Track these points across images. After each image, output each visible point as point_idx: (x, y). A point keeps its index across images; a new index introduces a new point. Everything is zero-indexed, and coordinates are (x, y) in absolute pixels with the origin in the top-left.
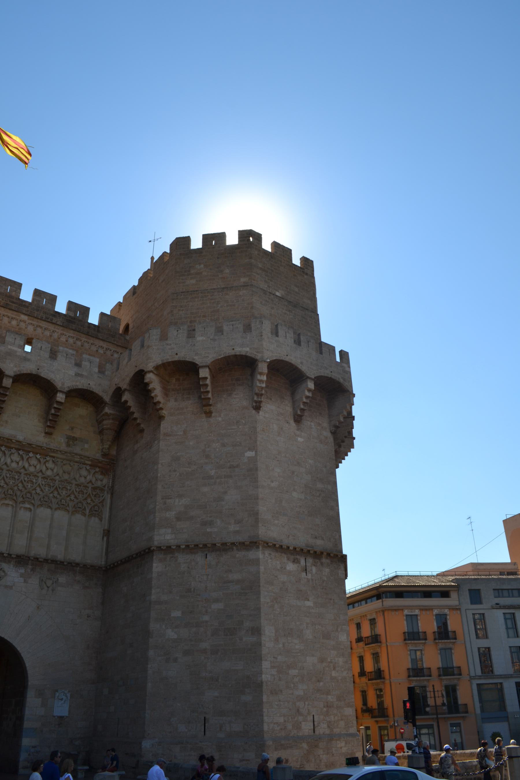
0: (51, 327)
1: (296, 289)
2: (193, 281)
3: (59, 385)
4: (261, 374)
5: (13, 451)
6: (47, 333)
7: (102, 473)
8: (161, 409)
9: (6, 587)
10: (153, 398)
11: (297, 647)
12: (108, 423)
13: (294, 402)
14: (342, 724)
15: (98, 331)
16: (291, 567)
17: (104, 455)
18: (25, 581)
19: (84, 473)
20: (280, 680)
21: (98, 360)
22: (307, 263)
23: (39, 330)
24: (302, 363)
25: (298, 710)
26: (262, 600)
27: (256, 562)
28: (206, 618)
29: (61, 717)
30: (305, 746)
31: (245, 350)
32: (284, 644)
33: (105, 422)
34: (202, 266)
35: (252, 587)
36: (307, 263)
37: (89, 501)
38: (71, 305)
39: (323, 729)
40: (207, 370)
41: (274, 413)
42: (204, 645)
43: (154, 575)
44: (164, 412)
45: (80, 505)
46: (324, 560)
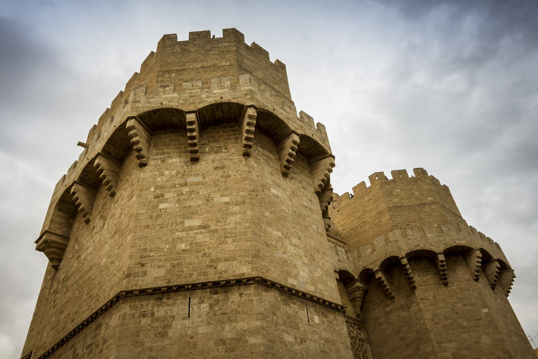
2: (398, 200)
7: (359, 329)
8: (414, 282)
10: (408, 274)
12: (359, 294)
13: (487, 277)
31: (463, 242)
33: (357, 293)
34: (399, 190)
44: (416, 284)
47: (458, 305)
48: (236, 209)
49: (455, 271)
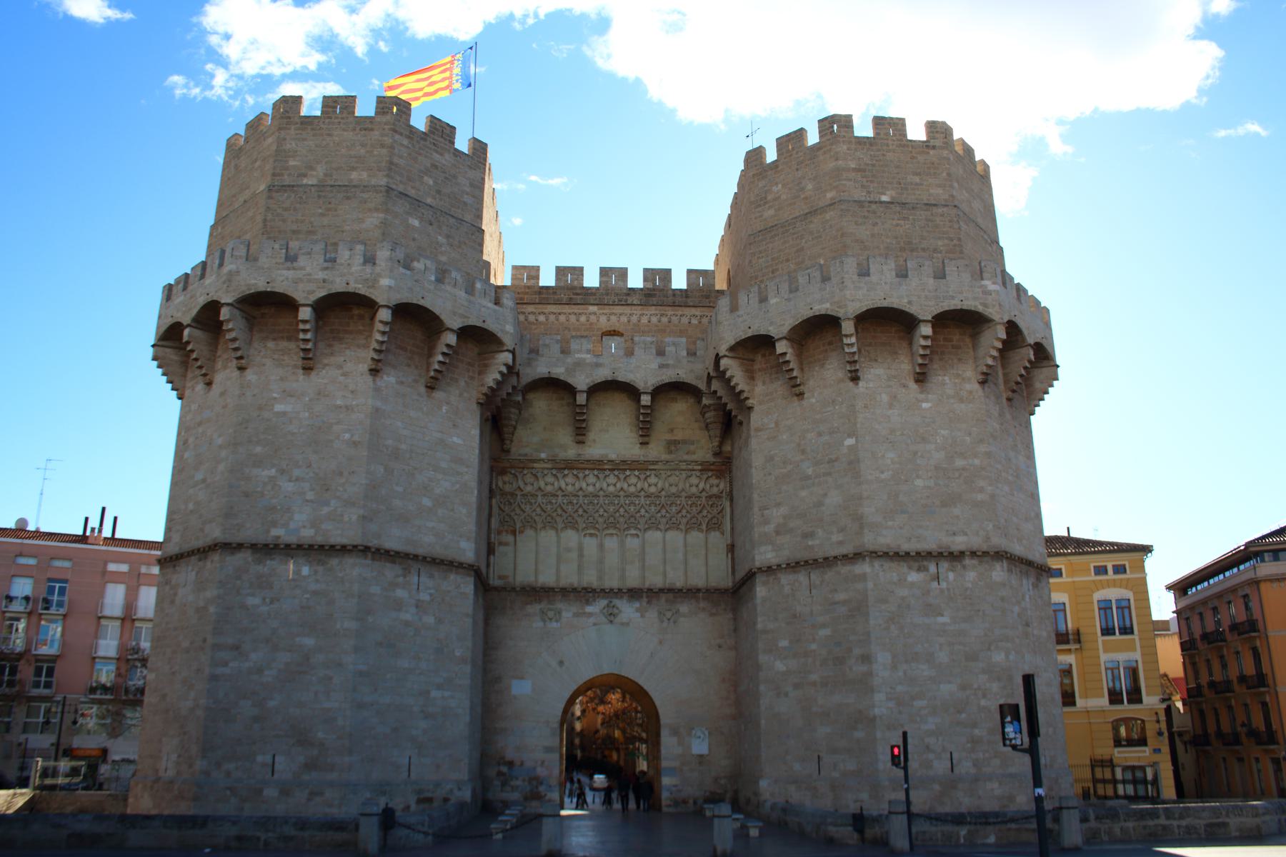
0: (627, 310)
1: (917, 179)
2: (771, 212)
3: (640, 385)
4: (851, 335)
5: (607, 473)
6: (624, 319)
7: (718, 477)
8: (747, 398)
9: (622, 624)
11: (926, 673)
14: (997, 762)
15: (687, 297)
16: (914, 577)
17: (716, 454)
18: (642, 616)
19: (694, 480)
20: (900, 713)
21: (684, 340)
22: (938, 130)
23: (613, 318)
24: (910, 302)
25: (928, 747)
26: (872, 622)
27: (863, 577)
28: (814, 646)
29: (701, 756)
30: (937, 787)
32: (905, 673)
33: (707, 415)
35: (859, 608)
36: (938, 130)
37: (705, 513)
38: (649, 274)
39: (965, 767)
40: (784, 342)
41: (885, 377)
42: (814, 677)
43: (758, 601)
44: (750, 402)
45: (694, 520)
46: (967, 561)
47: (809, 436)
48: (223, 454)
49: (823, 365)
